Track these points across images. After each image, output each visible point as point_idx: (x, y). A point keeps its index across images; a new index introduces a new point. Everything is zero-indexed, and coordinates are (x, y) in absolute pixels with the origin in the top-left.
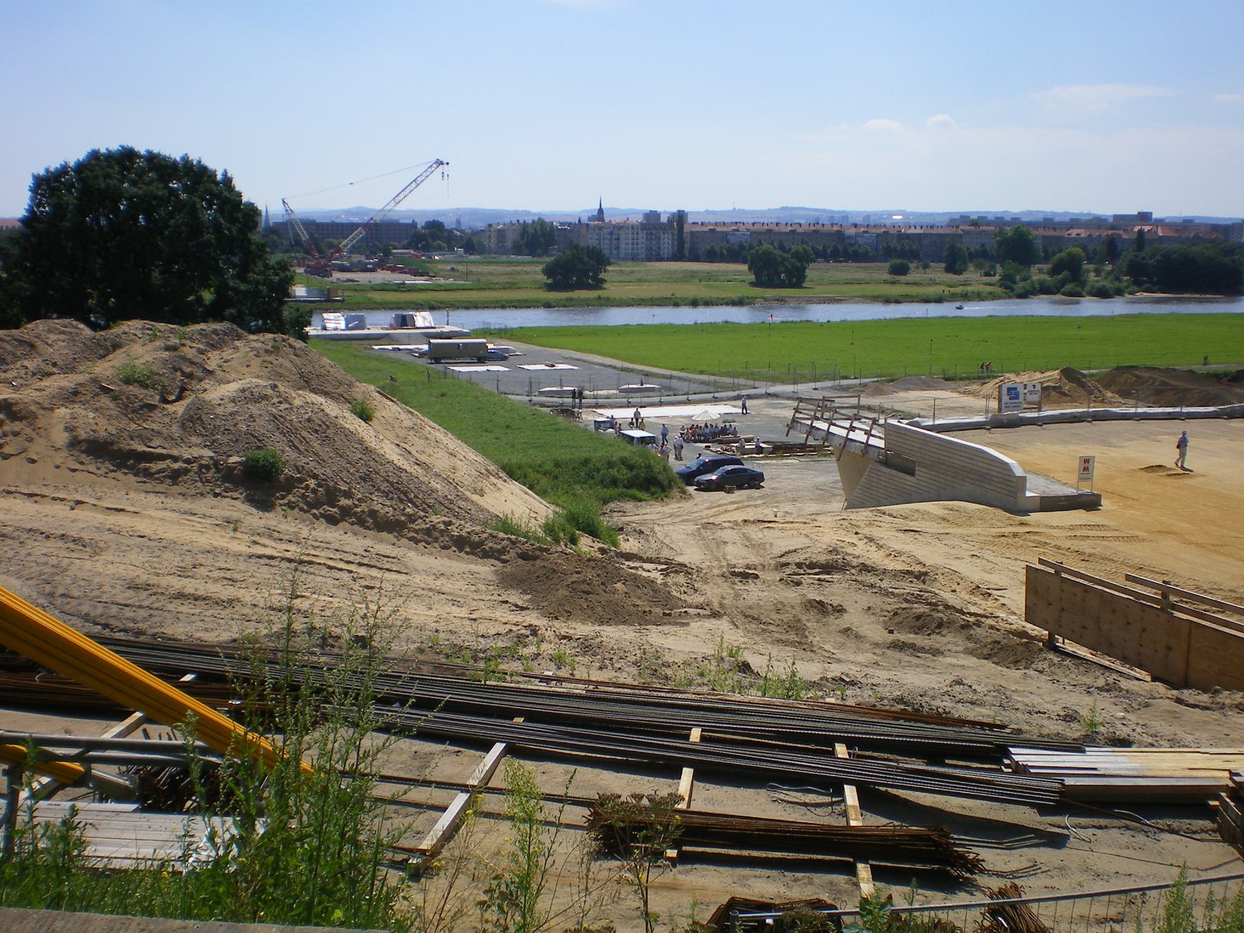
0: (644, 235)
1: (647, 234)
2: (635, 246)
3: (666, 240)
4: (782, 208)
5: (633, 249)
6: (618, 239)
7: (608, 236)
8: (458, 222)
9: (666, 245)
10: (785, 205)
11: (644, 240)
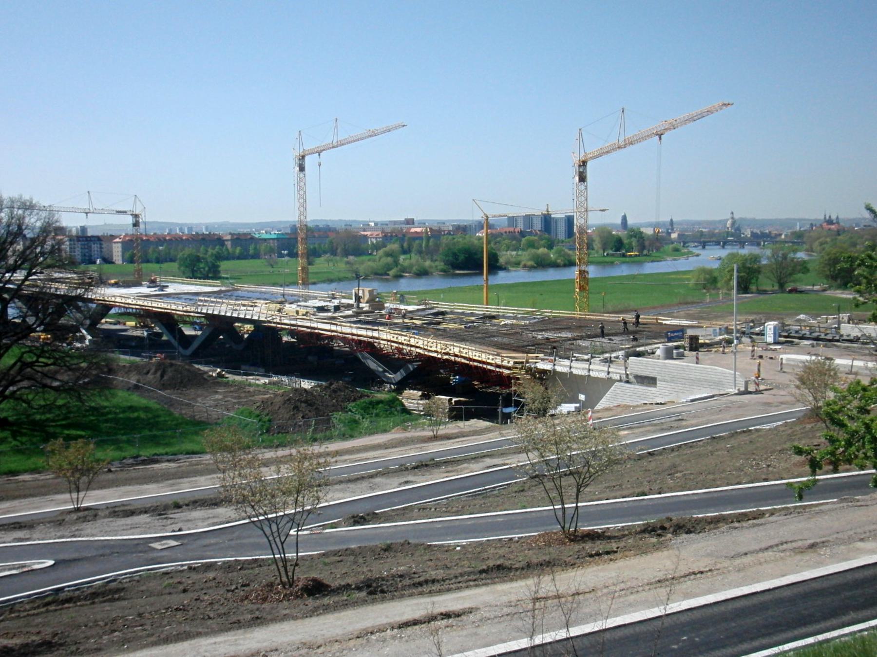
3: (96, 249)
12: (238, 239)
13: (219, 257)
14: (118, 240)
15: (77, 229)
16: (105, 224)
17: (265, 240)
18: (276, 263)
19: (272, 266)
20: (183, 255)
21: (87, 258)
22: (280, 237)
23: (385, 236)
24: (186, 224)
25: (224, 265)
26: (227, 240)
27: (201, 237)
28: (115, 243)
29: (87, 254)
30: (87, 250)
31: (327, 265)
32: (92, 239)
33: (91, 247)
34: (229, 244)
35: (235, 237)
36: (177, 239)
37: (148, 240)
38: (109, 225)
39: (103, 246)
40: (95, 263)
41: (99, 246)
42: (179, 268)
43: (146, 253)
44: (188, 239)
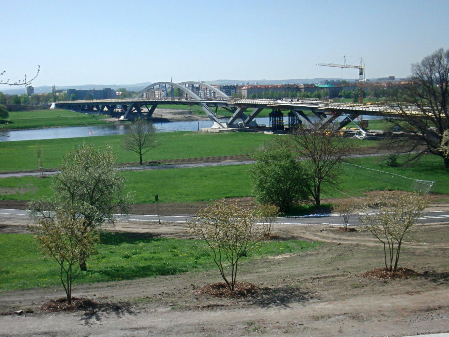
1: (226, 90)
12: (308, 87)
14: (244, 88)
23: (388, 86)
26: (302, 88)
28: (243, 89)
32: (231, 87)
34: (303, 90)
35: (306, 86)
36: (275, 88)
44: (280, 88)
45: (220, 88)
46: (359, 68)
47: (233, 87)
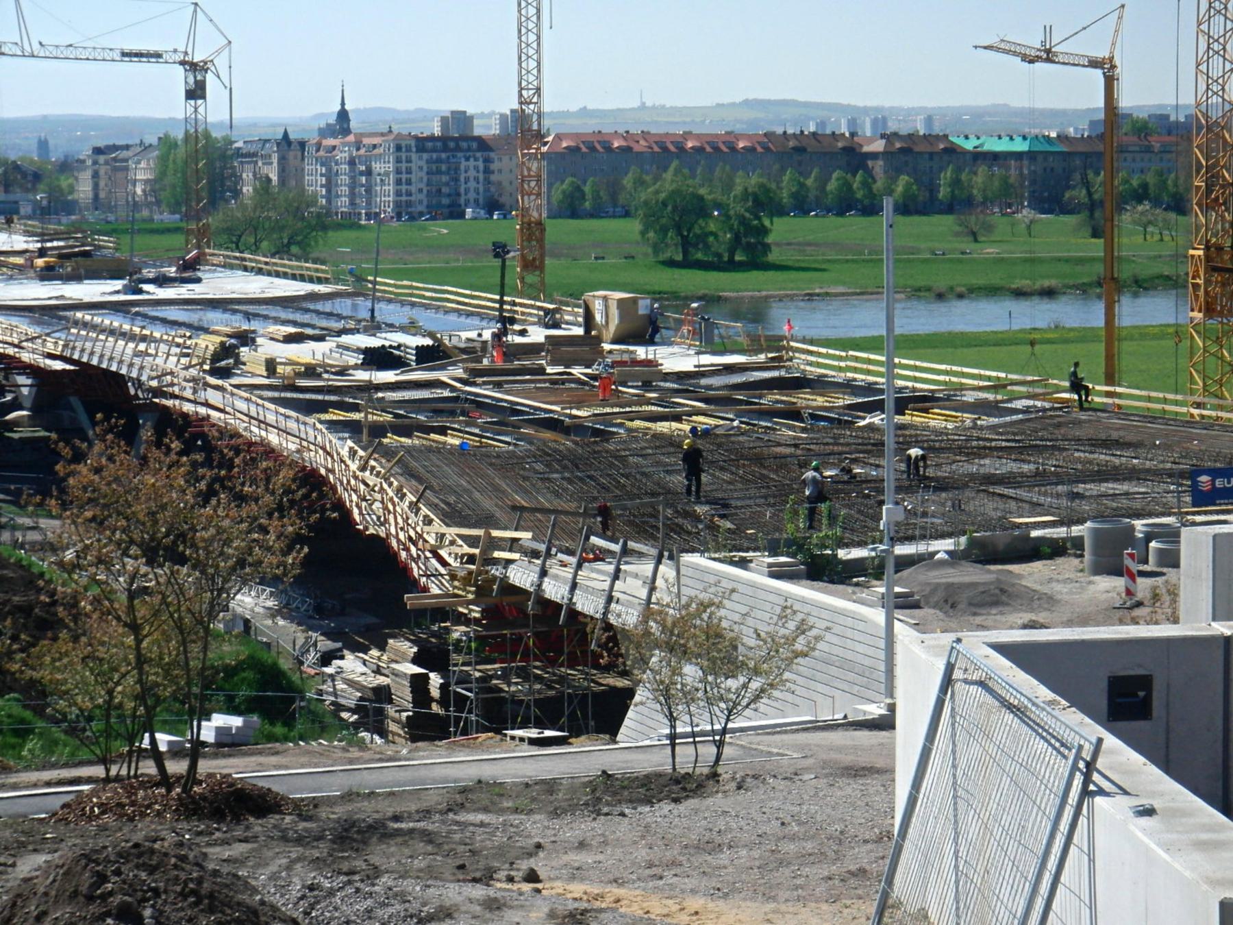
0: (423, 163)
1: (428, 162)
2: (404, 188)
3: (472, 173)
4: (746, 103)
5: (398, 193)
6: (369, 172)
7: (345, 167)
8: (43, 145)
9: (472, 184)
10: (751, 97)
11: (423, 174)
12: (904, 151)
13: (765, 203)
15: (503, 117)
16: (643, 107)
17: (995, 157)
18: (989, 228)
19: (975, 236)
20: (657, 192)
21: (445, 201)
22: (1039, 147)
24: (866, 110)
25: (781, 229)
26: (874, 156)
27: (791, 144)
29: (445, 190)
30: (445, 178)
31: (1140, 239)
32: (464, 145)
33: (457, 169)
34: (878, 167)
35: (898, 145)
36: (717, 149)
37: (627, 150)
38: (654, 107)
39: (494, 166)
40: (461, 215)
41: (481, 164)
42: (643, 233)
43: (614, 189)
44: (752, 150)
45: (398, 148)
46: (183, 63)
47: (475, 145)
